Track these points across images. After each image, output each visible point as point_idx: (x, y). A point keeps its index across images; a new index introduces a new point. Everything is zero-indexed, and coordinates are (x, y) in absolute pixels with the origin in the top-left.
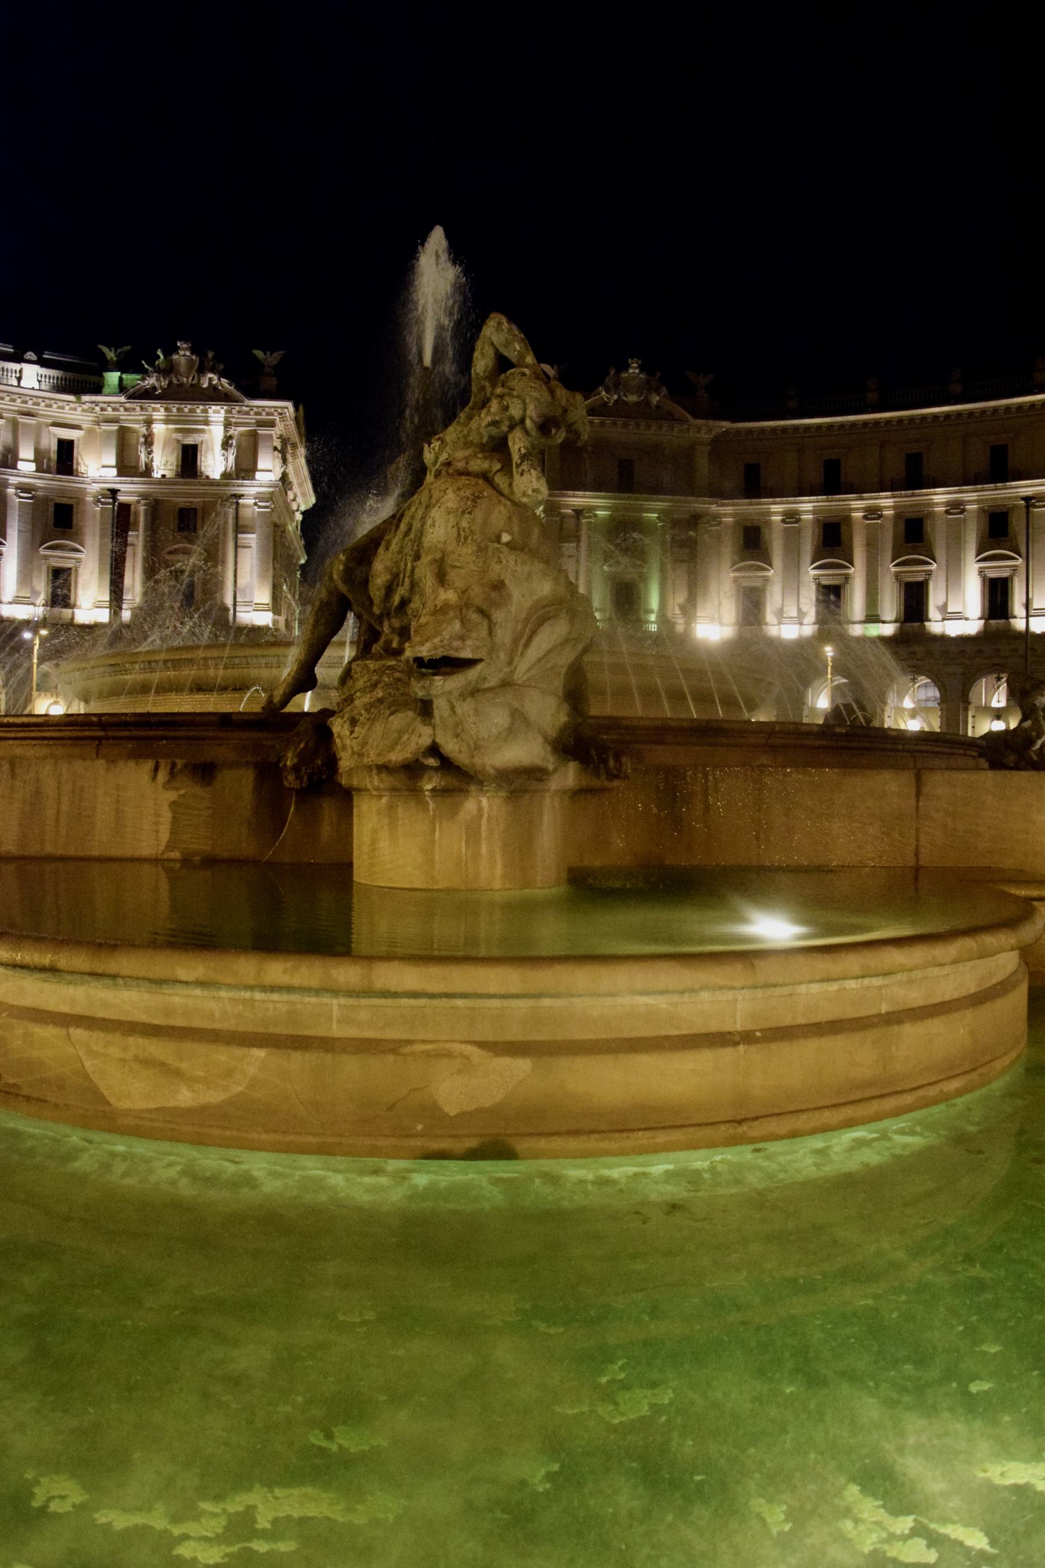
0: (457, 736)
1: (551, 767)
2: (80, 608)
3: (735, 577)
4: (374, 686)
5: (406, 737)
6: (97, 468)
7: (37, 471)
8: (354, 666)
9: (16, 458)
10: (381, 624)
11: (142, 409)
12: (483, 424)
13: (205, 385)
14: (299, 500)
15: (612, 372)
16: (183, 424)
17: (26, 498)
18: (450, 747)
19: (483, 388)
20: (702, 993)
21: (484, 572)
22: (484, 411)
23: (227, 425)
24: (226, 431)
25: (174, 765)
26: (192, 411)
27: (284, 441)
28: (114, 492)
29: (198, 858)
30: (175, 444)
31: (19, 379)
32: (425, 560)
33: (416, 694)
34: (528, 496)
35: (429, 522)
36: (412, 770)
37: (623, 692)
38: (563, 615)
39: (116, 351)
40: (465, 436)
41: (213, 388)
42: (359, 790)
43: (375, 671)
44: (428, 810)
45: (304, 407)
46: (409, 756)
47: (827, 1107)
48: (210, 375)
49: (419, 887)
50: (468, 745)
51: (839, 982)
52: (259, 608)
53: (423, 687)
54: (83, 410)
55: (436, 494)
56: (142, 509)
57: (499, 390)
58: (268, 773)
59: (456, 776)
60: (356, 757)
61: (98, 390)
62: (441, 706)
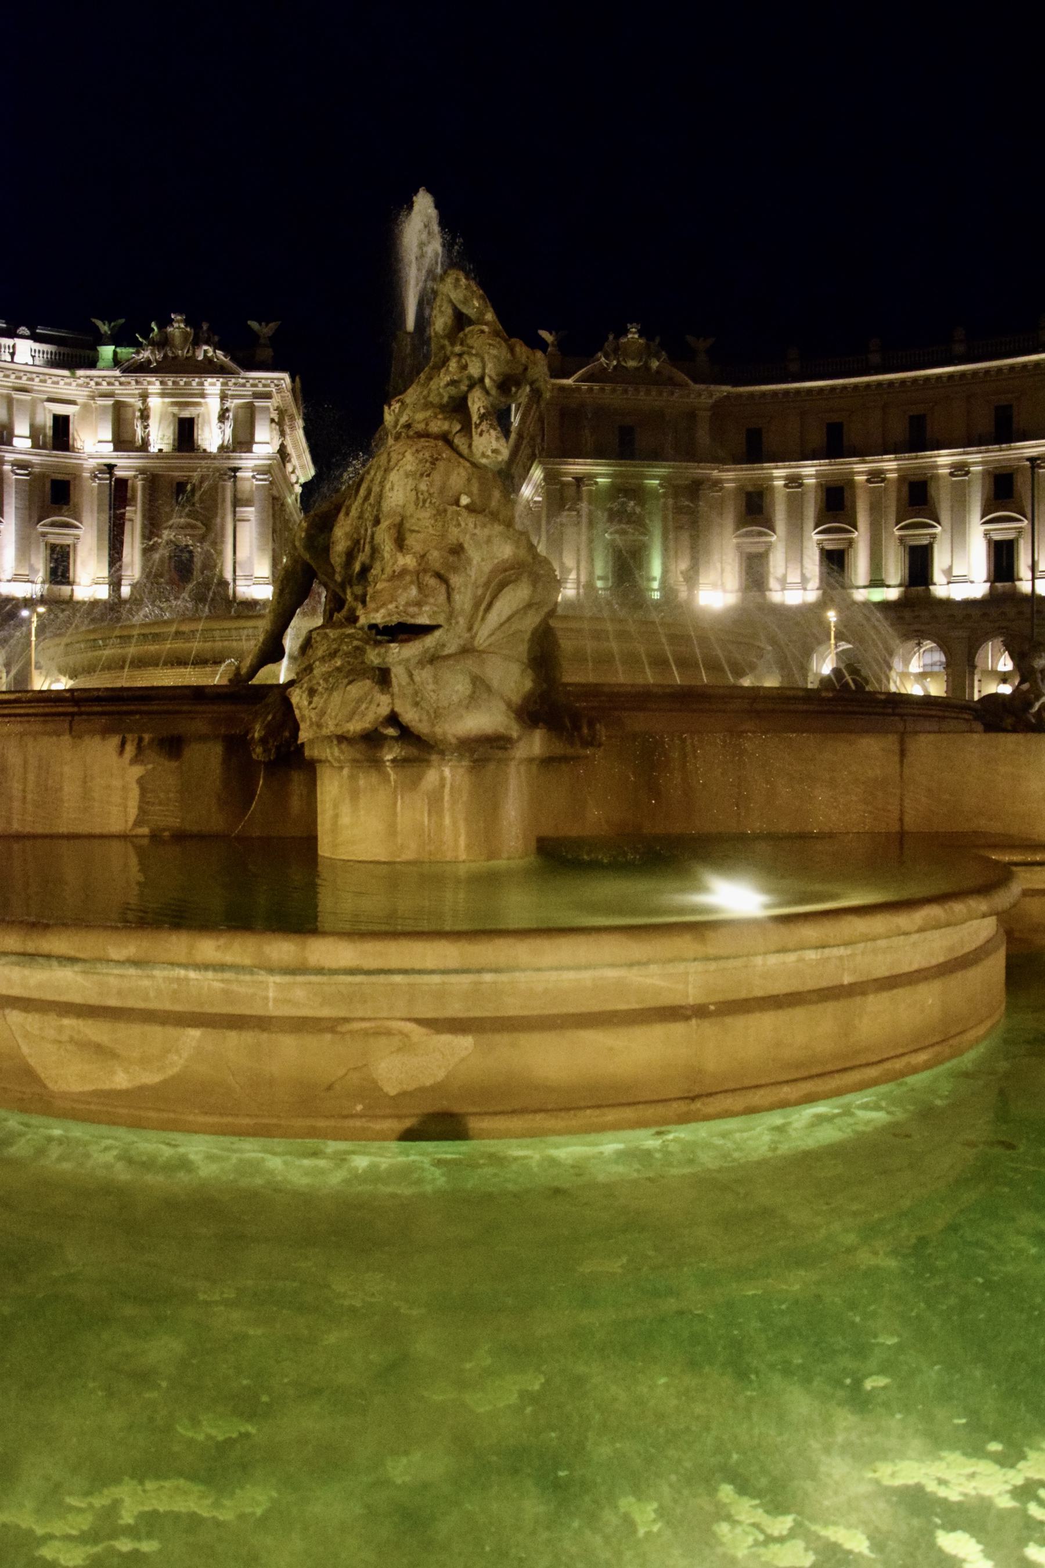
0: (416, 704)
1: (515, 735)
2: (79, 585)
3: (738, 543)
4: (333, 655)
5: (364, 706)
6: (93, 443)
7: (32, 447)
8: (314, 635)
9: (11, 435)
10: (345, 594)
11: (137, 382)
12: (442, 384)
13: (201, 358)
14: (298, 472)
16: (182, 398)
17: (22, 475)
18: (409, 716)
19: (443, 347)
20: (652, 966)
21: (443, 536)
22: (443, 370)
23: (223, 397)
24: (222, 404)
25: (141, 740)
26: (186, 383)
27: (281, 412)
28: (111, 468)
29: (166, 834)
30: (171, 418)
31: (13, 355)
32: (384, 524)
33: (372, 662)
34: (488, 457)
35: (388, 486)
36: (372, 739)
37: (604, 660)
38: (525, 578)
39: (110, 324)
40: (425, 398)
41: (208, 360)
42: (320, 761)
43: (334, 640)
44: (389, 781)
45: (301, 378)
46: (368, 725)
47: (787, 1082)
48: (205, 347)
49: (383, 860)
50: (428, 712)
51: (799, 953)
52: (258, 581)
53: (379, 655)
54: (78, 385)
55: (394, 457)
56: (139, 484)
57: (458, 349)
58: (236, 745)
59: (417, 746)
60: (315, 728)
61: (92, 364)
62: (399, 675)
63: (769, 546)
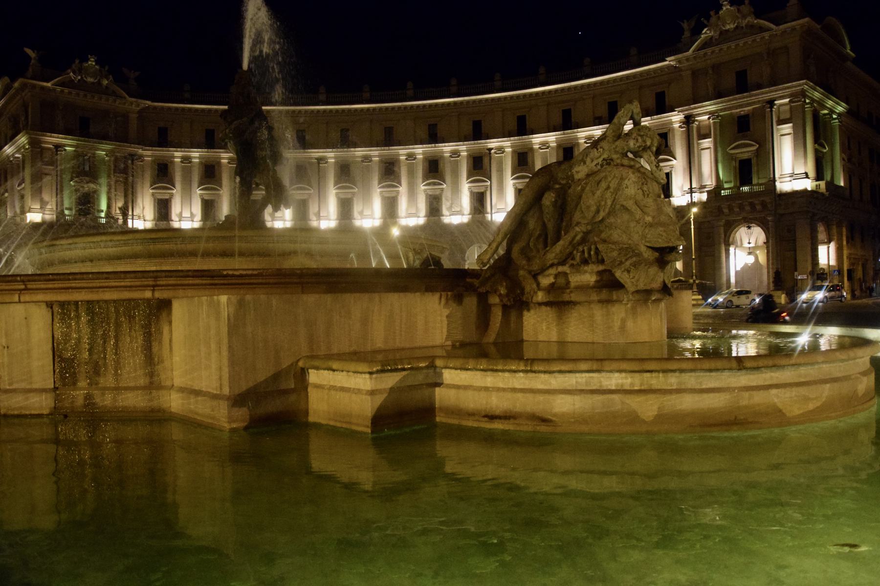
15: (77, 61)
63: (172, 195)
